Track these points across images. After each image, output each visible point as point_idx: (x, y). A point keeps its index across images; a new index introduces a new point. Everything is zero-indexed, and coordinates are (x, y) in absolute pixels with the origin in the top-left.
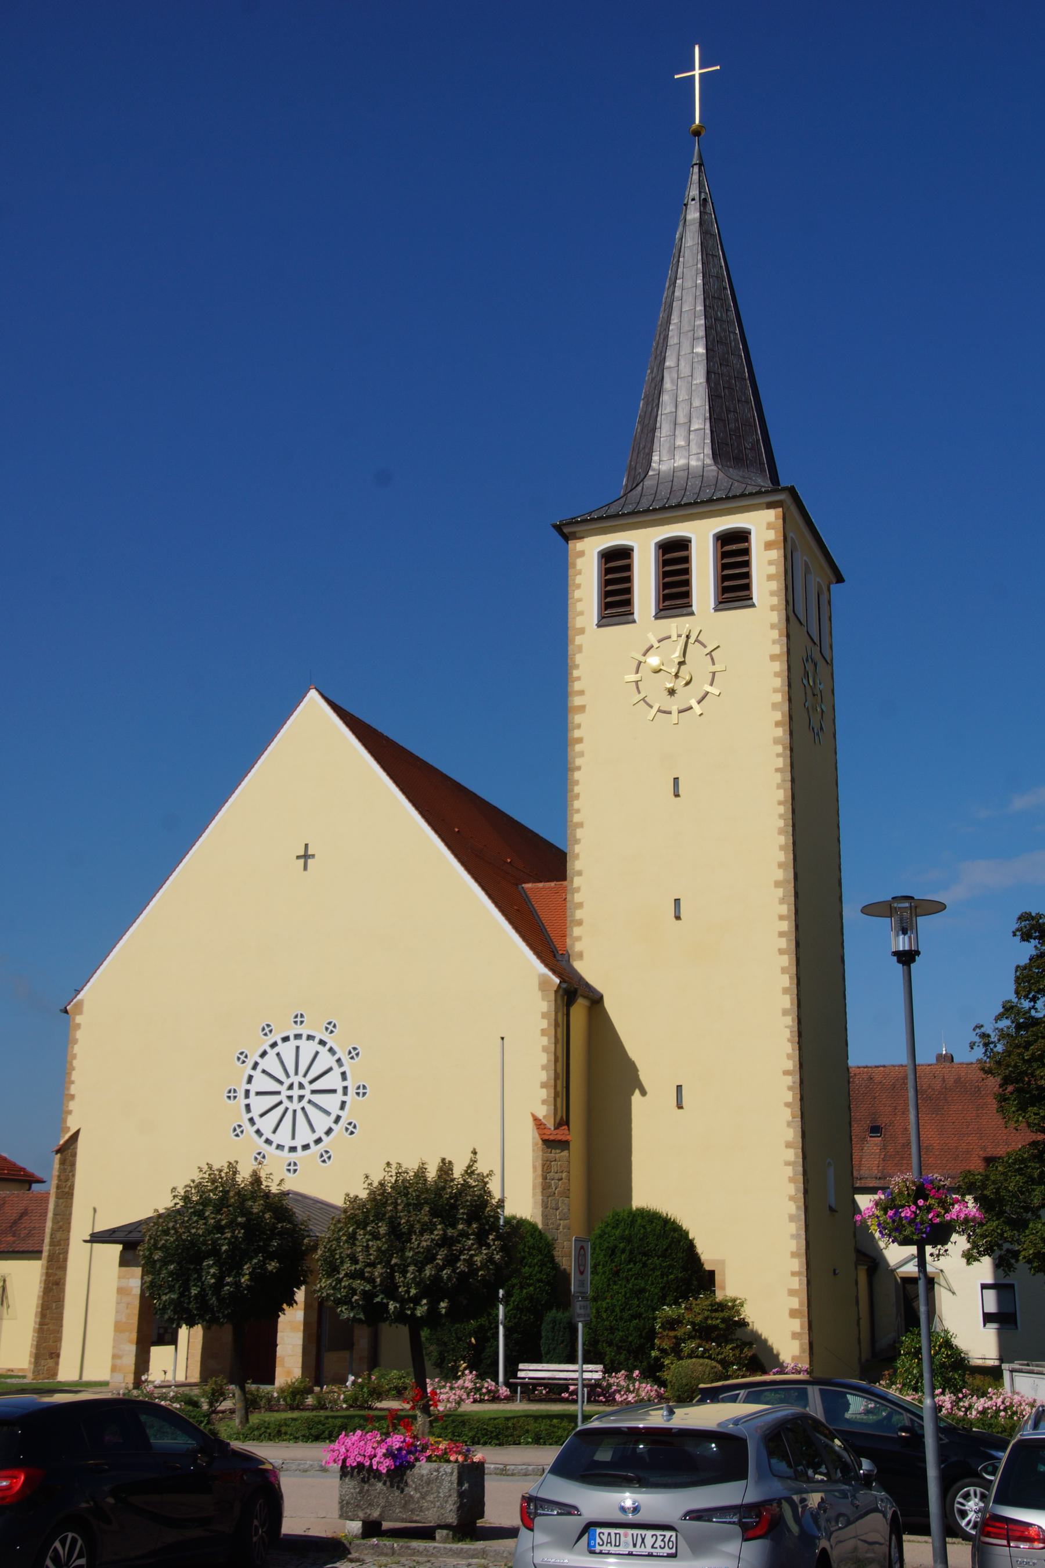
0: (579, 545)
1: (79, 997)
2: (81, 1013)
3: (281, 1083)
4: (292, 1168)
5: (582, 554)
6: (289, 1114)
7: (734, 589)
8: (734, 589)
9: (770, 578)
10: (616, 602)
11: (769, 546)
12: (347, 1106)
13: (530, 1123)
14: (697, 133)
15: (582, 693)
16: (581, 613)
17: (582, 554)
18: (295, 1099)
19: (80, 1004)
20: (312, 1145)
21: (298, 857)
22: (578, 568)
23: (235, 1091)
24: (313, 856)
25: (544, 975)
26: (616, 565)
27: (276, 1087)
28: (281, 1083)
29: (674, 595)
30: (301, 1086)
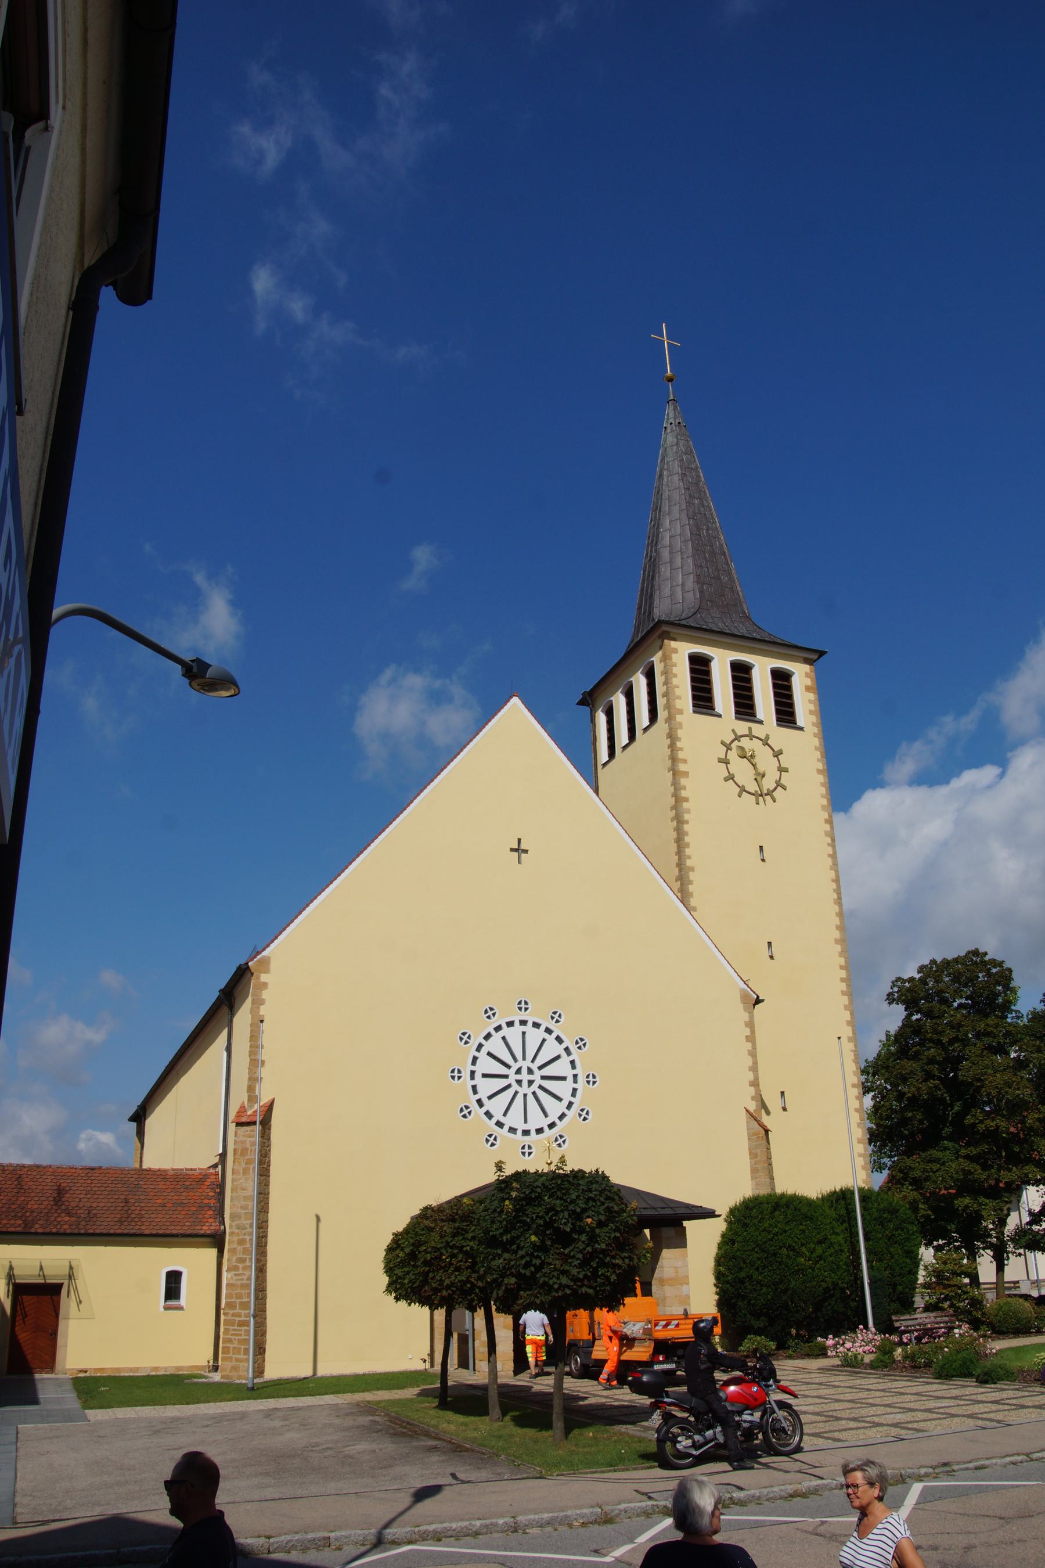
0: (673, 644)
1: (264, 953)
2: (267, 971)
3: (508, 1067)
4: (526, 1151)
5: (676, 651)
6: (519, 1098)
7: (786, 714)
8: (786, 714)
9: (811, 712)
10: (703, 699)
11: (808, 689)
12: (578, 1093)
13: (744, 1114)
14: (670, 380)
15: (685, 761)
16: (679, 698)
17: (676, 651)
18: (525, 1083)
19: (266, 961)
20: (546, 1129)
21: (512, 850)
22: (674, 660)
23: (459, 1071)
24: (526, 851)
25: (742, 991)
26: (700, 666)
27: (503, 1070)
28: (508, 1067)
29: (745, 707)
30: (530, 1071)
